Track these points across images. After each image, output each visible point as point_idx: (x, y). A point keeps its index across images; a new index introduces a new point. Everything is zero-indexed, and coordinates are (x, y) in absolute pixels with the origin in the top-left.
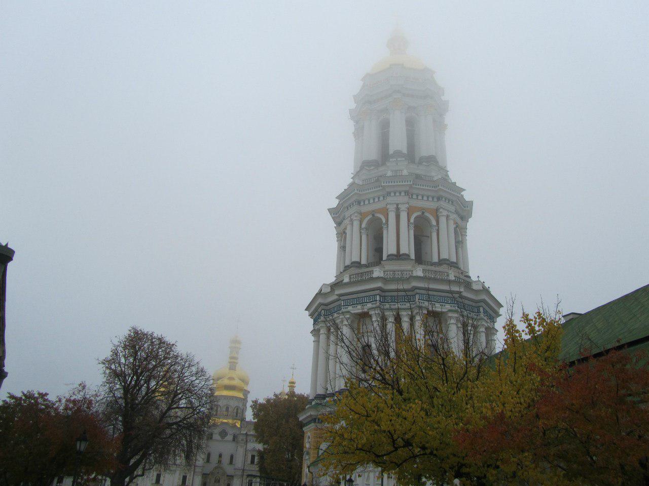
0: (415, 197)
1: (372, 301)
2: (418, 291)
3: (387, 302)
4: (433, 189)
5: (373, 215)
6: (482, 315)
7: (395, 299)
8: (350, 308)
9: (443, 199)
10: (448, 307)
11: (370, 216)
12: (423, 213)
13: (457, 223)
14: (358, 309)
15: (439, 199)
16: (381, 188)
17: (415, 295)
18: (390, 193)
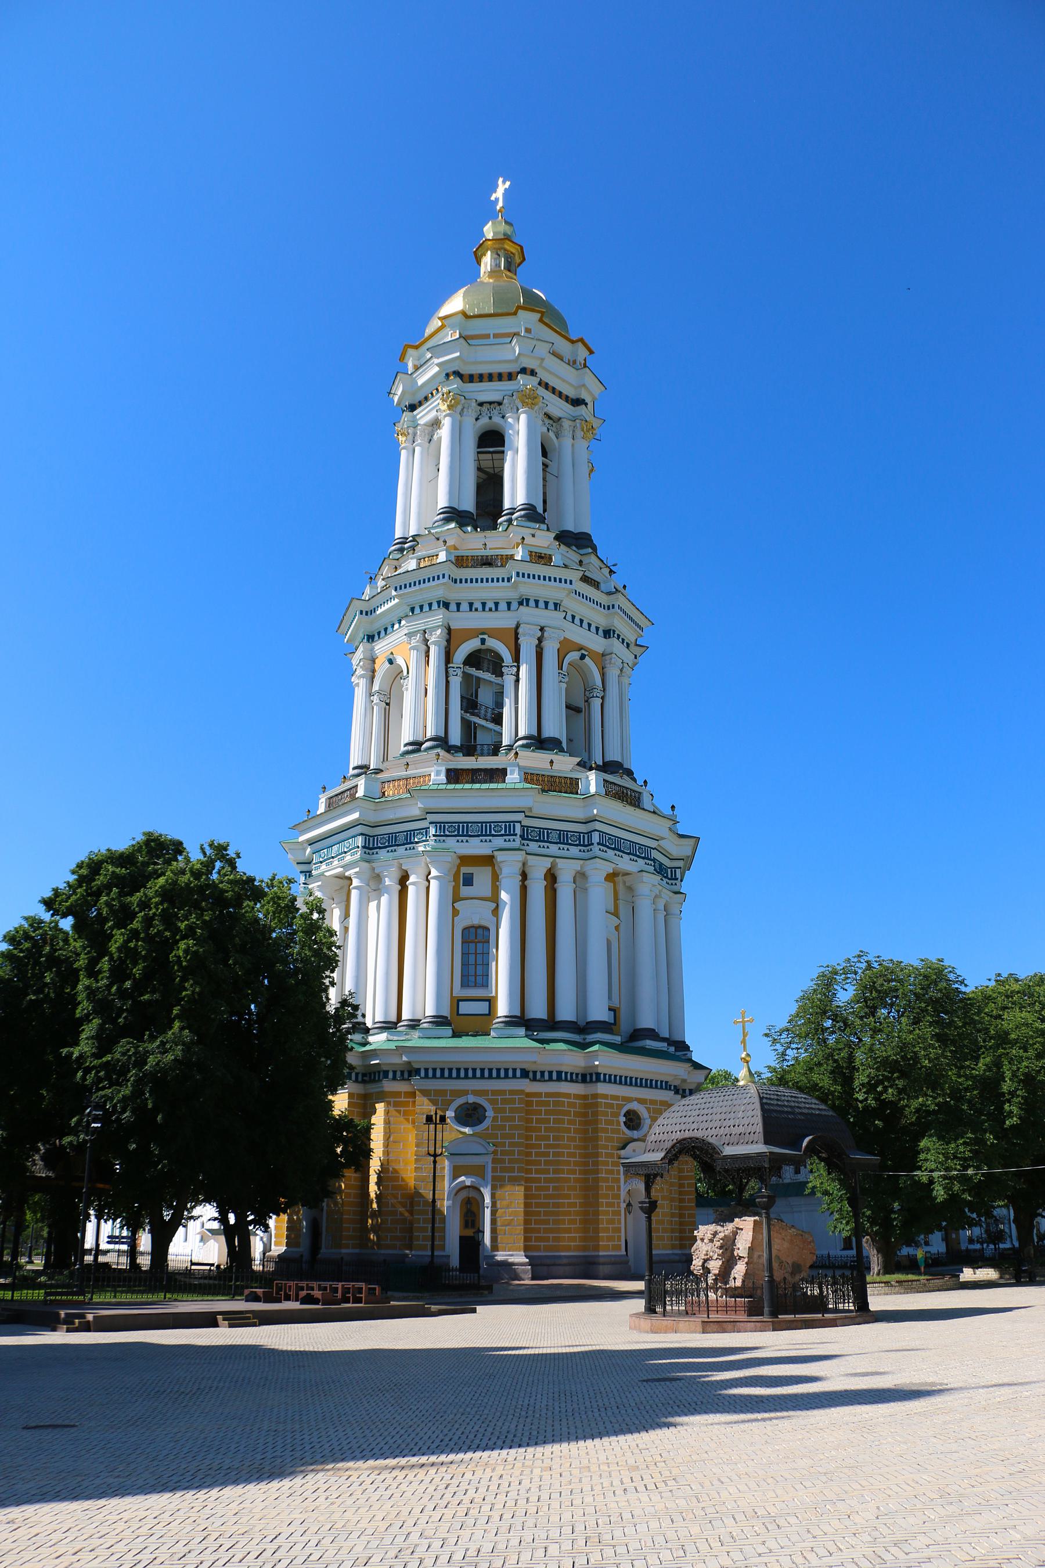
0: (465, 606)
1: (351, 850)
2: (431, 818)
3: (380, 848)
4: (506, 583)
5: (391, 662)
6: (596, 848)
7: (392, 842)
8: (324, 867)
9: (532, 603)
10: (499, 842)
11: (387, 665)
12: (483, 641)
13: (581, 648)
14: (333, 869)
15: (521, 603)
16: (397, 600)
17: (429, 828)
18: (412, 610)
